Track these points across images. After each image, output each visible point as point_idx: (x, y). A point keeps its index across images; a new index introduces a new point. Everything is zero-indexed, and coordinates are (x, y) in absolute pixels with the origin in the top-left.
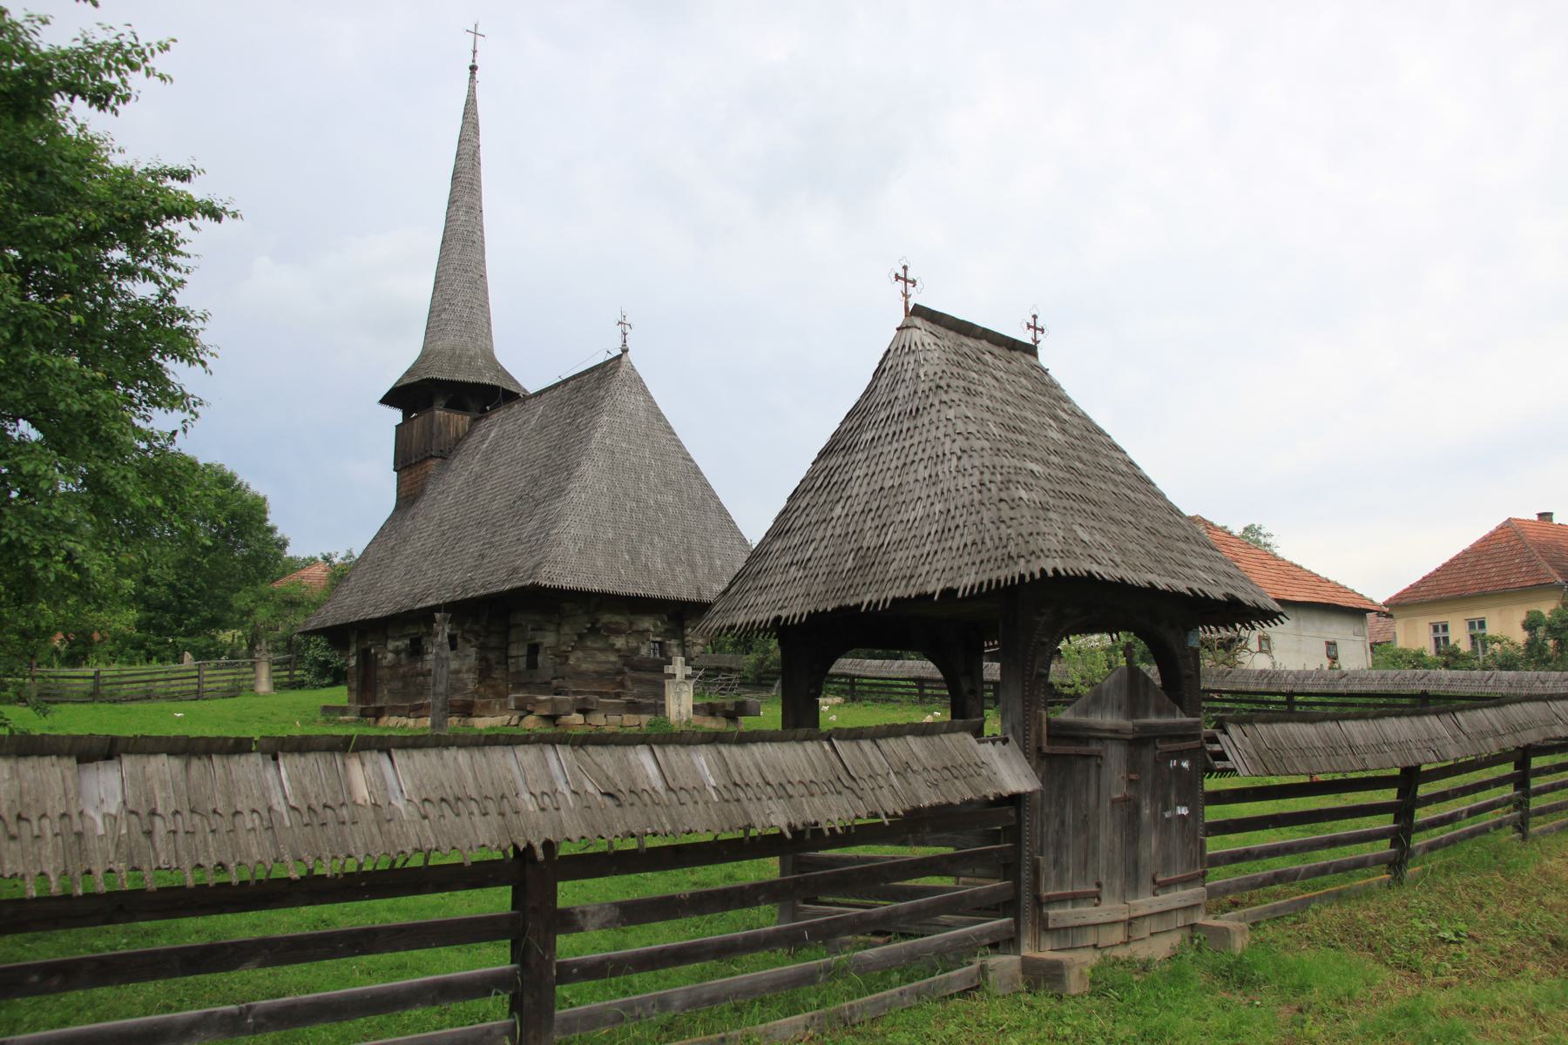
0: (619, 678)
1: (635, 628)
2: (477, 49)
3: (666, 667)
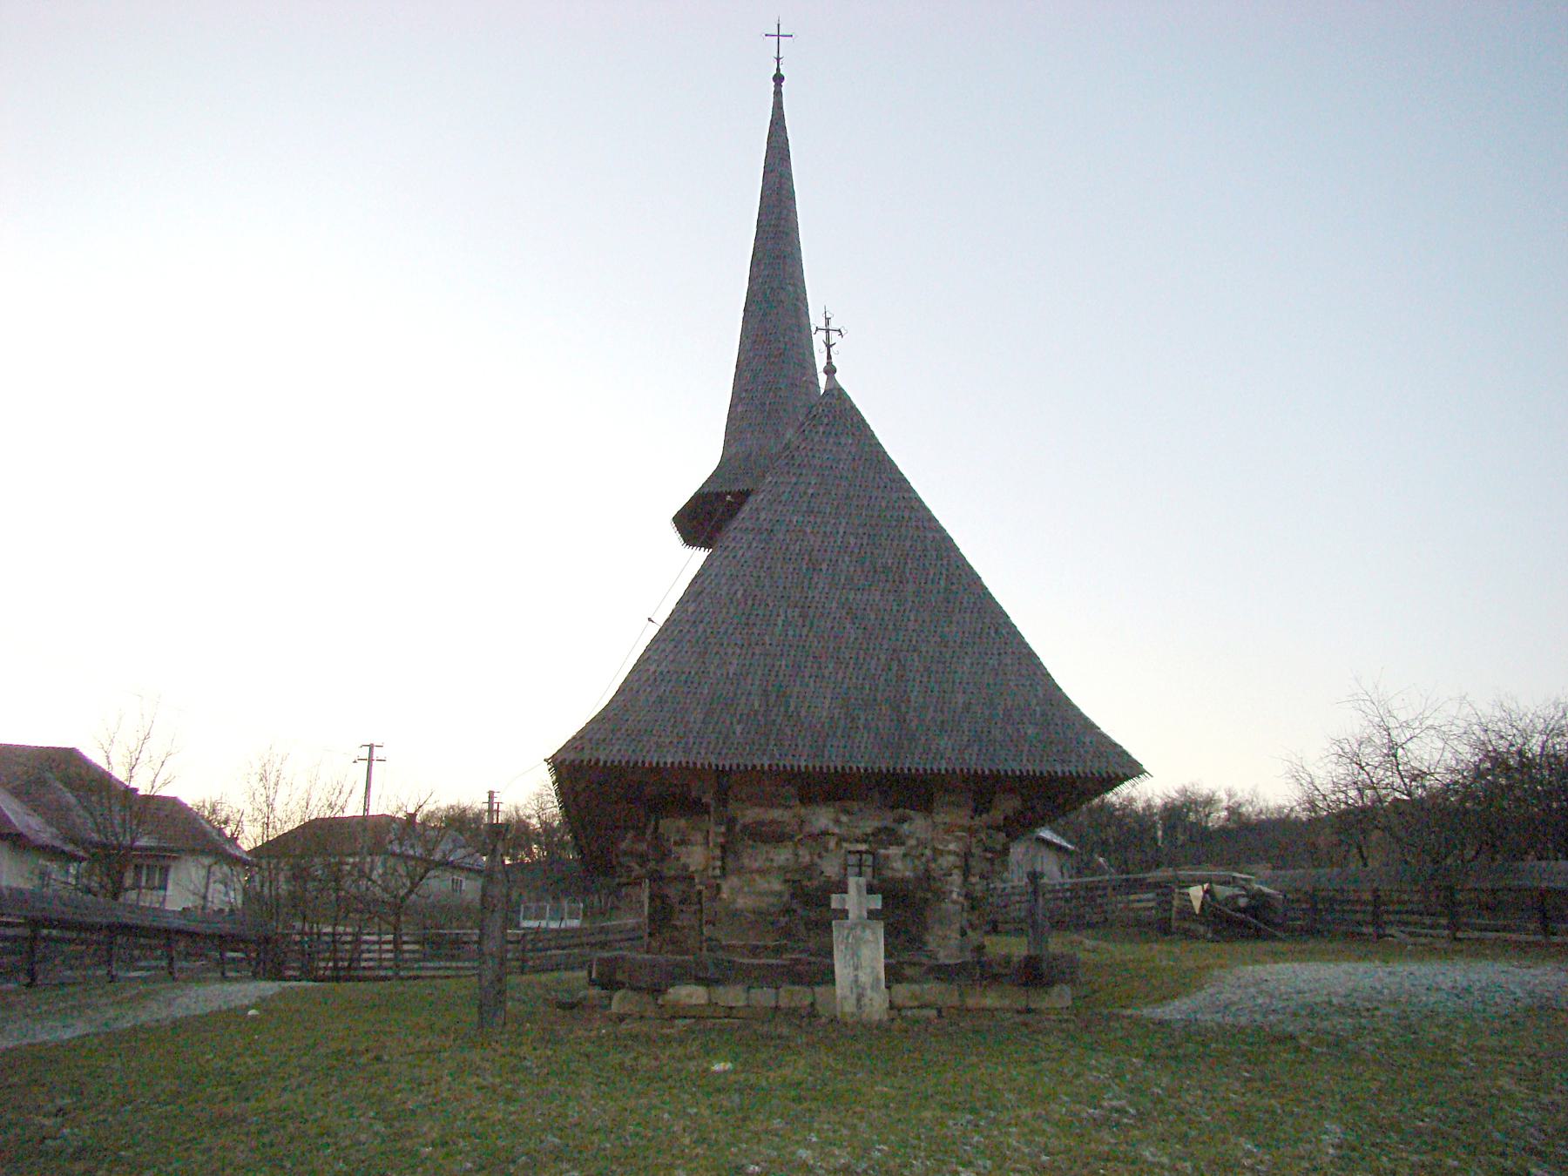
0: (783, 920)
1: (807, 829)
3: (834, 896)
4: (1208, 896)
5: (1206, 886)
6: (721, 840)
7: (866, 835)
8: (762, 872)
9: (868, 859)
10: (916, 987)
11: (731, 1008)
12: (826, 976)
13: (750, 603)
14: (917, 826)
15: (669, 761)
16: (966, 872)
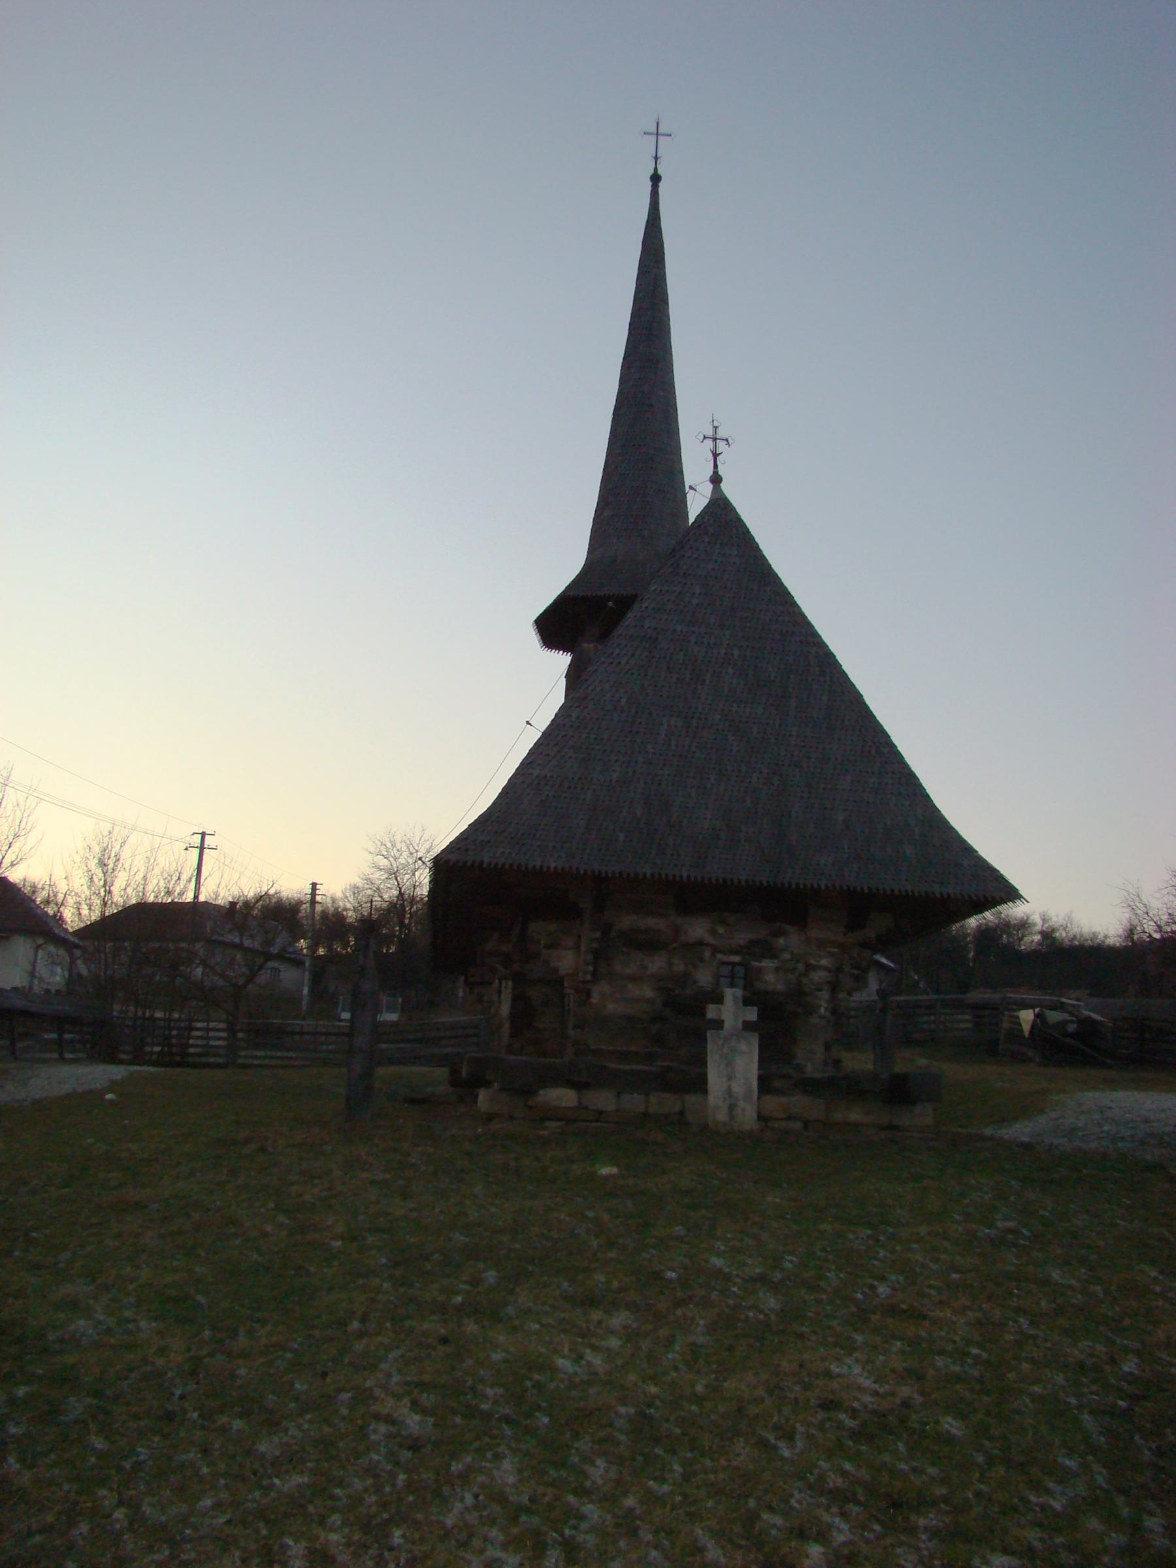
2: (659, 155)
4: (1039, 1021)
5: (1037, 1010)
6: (595, 945)
7: (740, 946)
8: (634, 979)
9: (740, 971)
10: (784, 1100)
11: (601, 1113)
12: (700, 1085)
13: (633, 710)
14: (791, 941)
15: (553, 865)
16: (834, 988)
